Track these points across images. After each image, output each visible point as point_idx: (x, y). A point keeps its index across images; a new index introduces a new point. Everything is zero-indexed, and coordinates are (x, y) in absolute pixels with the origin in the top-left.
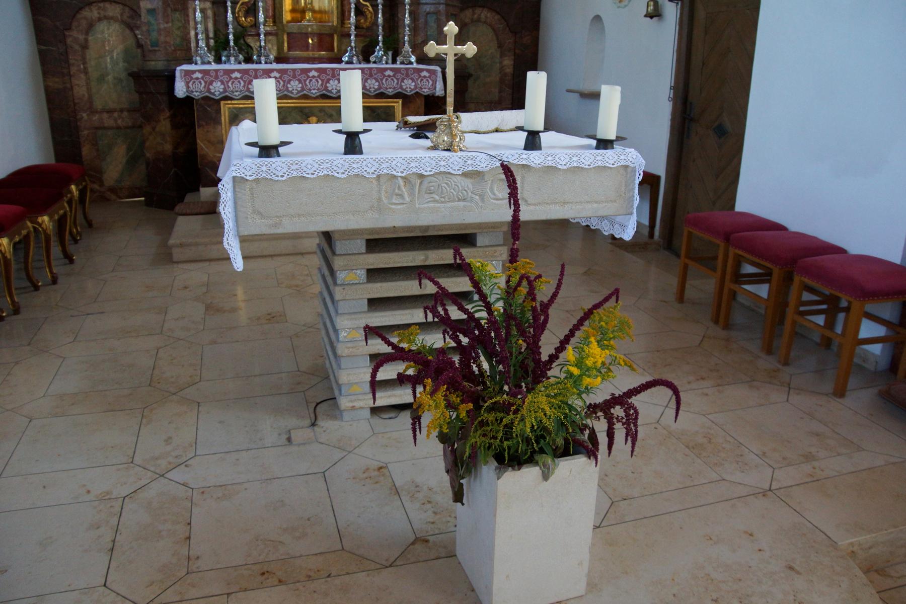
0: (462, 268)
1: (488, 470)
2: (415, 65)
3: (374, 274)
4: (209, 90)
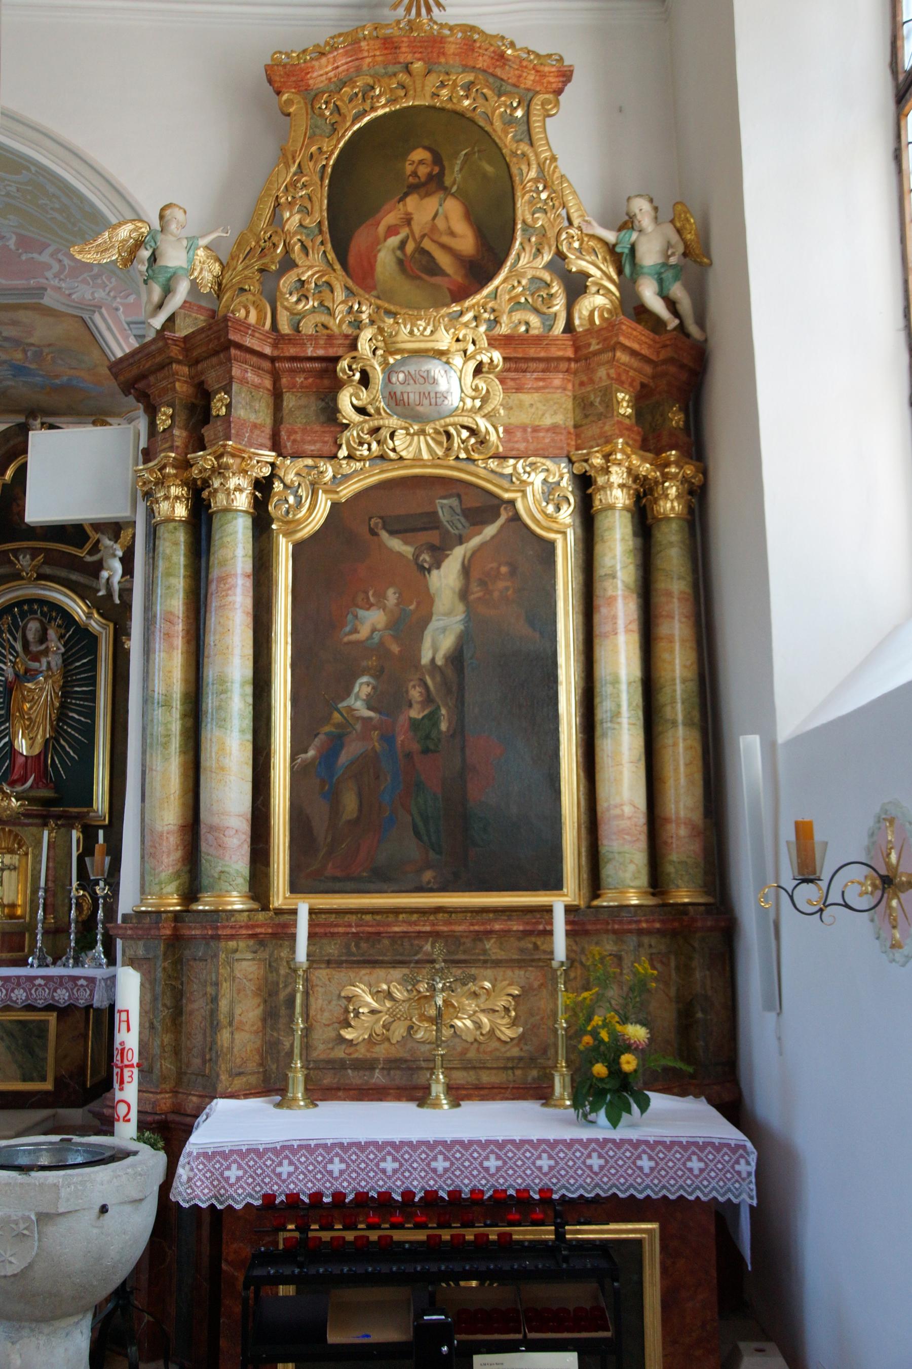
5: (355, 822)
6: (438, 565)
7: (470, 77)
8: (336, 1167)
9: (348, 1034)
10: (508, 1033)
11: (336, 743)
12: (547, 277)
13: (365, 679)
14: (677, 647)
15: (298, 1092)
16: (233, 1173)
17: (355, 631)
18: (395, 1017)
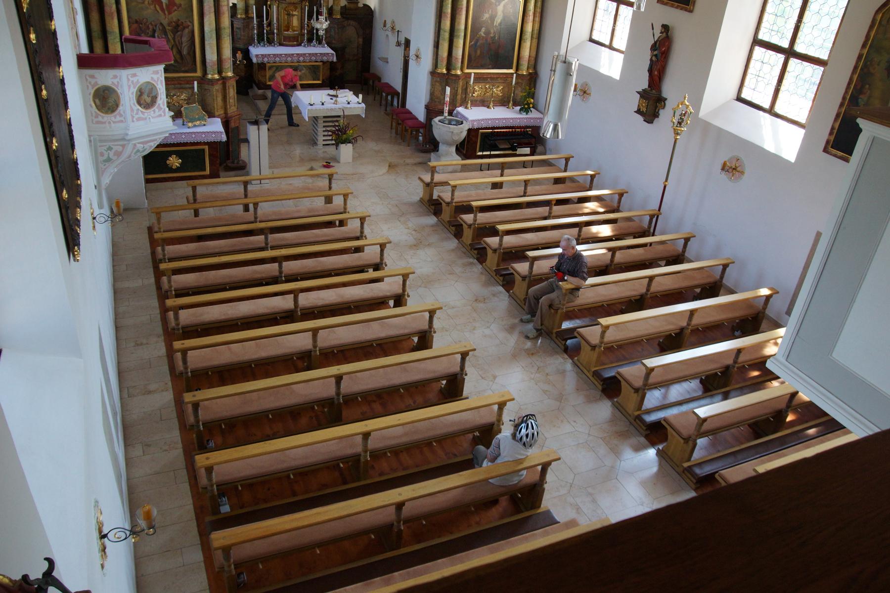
0: (337, 121)
1: (340, 144)
3: (324, 122)
4: (263, 60)
5: (479, 56)
6: (499, 5)
8: (490, 122)
9: (474, 95)
10: (501, 95)
11: (477, 41)
13: (484, 28)
14: (537, 22)
15: (469, 105)
16: (475, 123)
17: (483, 18)
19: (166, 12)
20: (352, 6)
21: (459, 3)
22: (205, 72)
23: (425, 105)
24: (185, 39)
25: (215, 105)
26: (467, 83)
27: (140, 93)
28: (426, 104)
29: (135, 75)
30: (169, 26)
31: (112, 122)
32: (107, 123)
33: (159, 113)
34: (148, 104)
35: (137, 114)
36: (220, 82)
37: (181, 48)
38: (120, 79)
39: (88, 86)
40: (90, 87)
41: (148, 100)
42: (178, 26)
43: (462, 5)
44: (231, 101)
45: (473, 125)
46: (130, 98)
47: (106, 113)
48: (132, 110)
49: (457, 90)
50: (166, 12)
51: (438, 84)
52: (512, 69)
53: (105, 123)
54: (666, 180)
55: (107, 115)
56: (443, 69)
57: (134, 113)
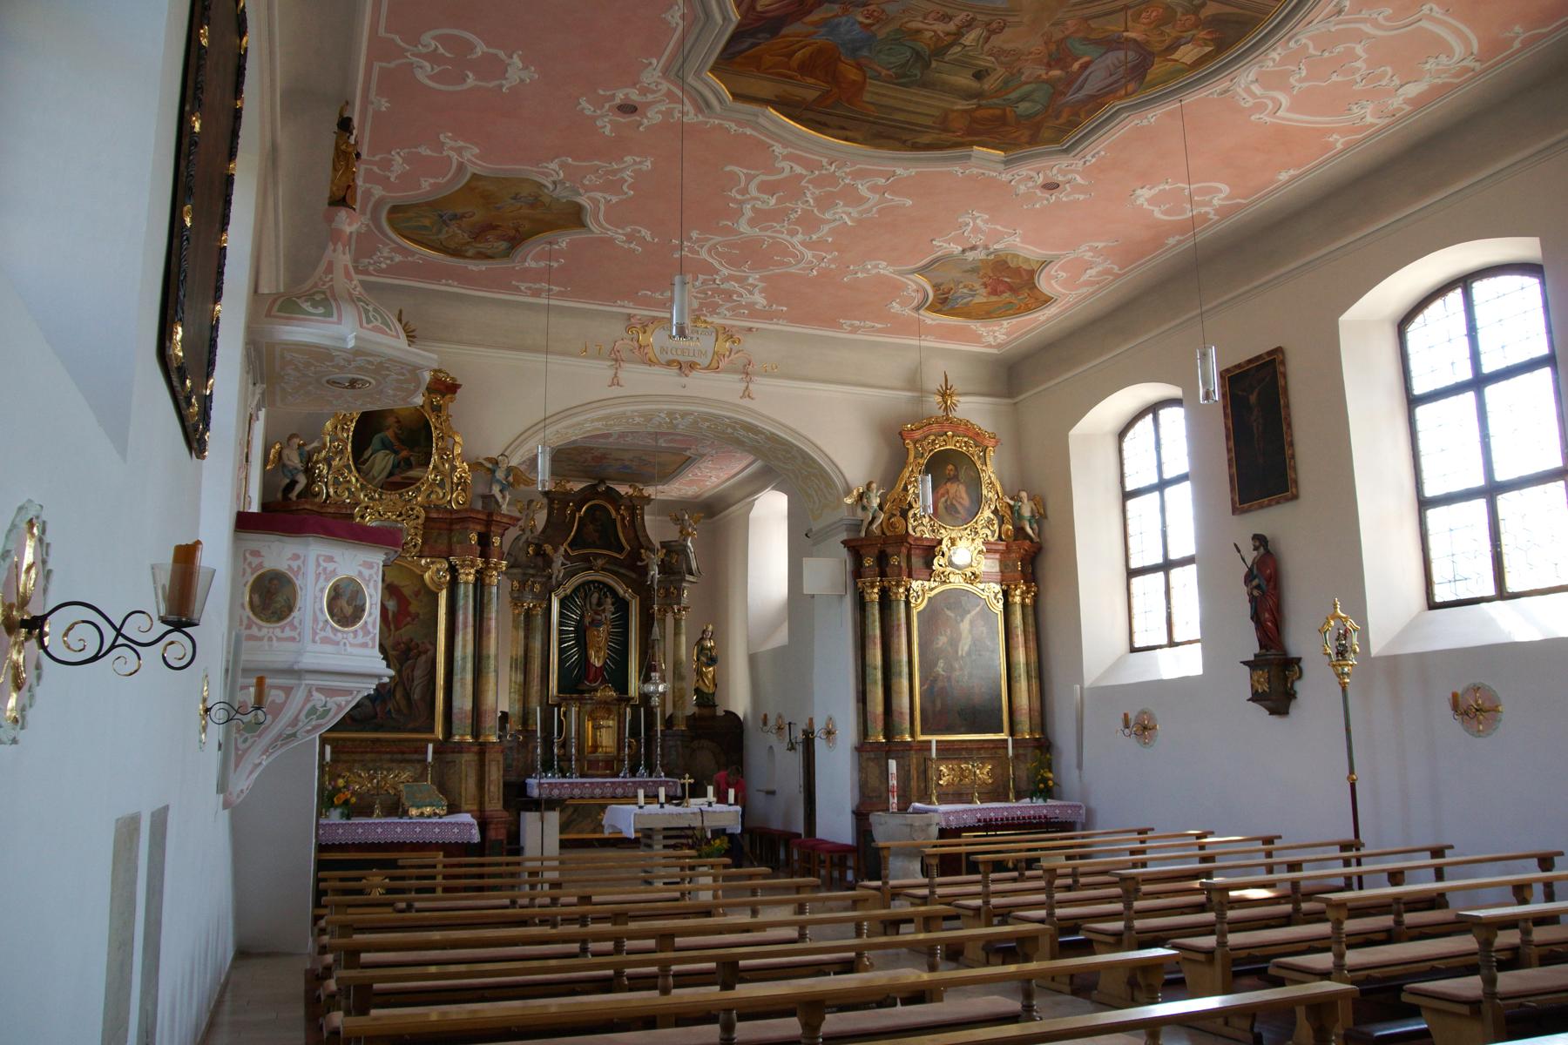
2: (664, 779)
6: (962, 621)
7: (966, 439)
9: (941, 782)
10: (990, 781)
12: (992, 516)
16: (951, 818)
18: (954, 776)
19: (392, 627)
20: (706, 712)
21: (894, 617)
22: (448, 731)
23: (853, 812)
24: (418, 673)
25: (463, 790)
26: (927, 759)
27: (336, 595)
28: (855, 809)
29: (330, 559)
30: (394, 649)
31: (274, 639)
32: (266, 639)
33: (364, 640)
34: (345, 617)
35: (323, 629)
36: (476, 749)
37: (411, 686)
38: (304, 562)
39: (244, 569)
40: (249, 571)
41: (349, 610)
42: (409, 649)
43: (899, 619)
44: (492, 788)
45: (947, 821)
46: (315, 598)
47: (268, 620)
48: (315, 620)
49: (909, 771)
50: (392, 627)
51: (871, 764)
52: (1002, 732)
53: (261, 639)
54: (1352, 771)
55: (268, 625)
56: (877, 737)
57: (319, 627)
